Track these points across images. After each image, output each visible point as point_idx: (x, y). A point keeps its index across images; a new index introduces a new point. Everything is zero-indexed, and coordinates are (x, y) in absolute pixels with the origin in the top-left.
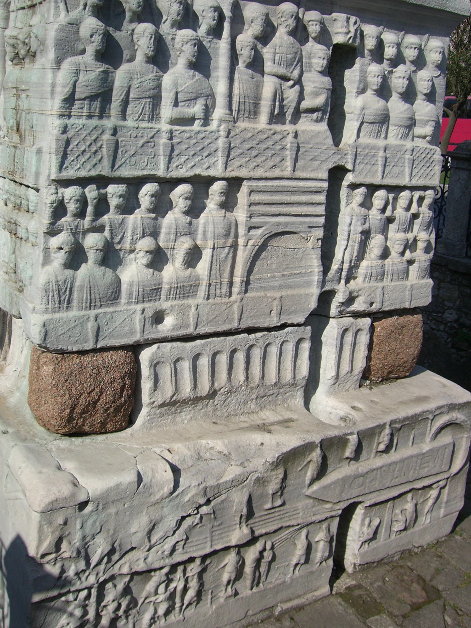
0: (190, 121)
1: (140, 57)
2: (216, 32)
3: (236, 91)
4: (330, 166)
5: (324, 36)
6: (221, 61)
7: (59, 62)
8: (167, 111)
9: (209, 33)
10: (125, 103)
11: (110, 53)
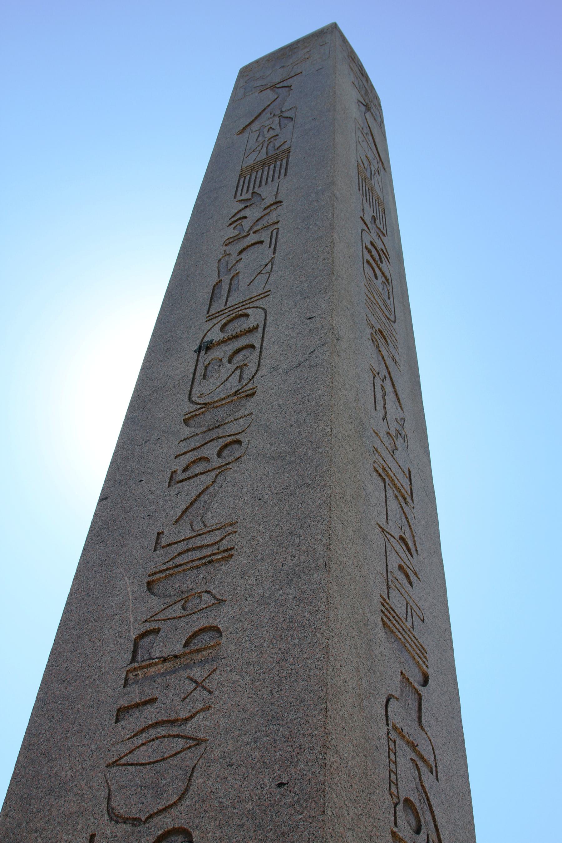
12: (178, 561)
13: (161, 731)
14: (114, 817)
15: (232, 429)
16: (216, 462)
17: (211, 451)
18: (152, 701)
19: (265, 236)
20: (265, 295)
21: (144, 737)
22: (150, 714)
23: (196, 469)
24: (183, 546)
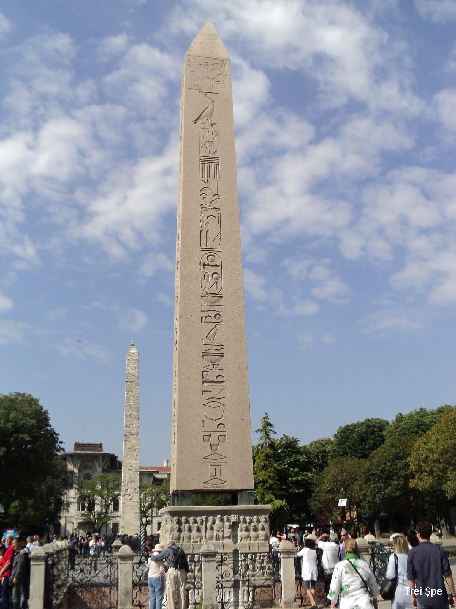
0: (197, 542)
1: (186, 531)
2: (202, 524)
3: (207, 535)
4: (233, 549)
5: (228, 520)
6: (203, 529)
7: (170, 533)
8: (192, 540)
9: (201, 524)
10: (183, 539)
11: (180, 530)
13: (213, 400)
15: (217, 309)
16: (214, 320)
17: (212, 314)
18: (211, 391)
22: (210, 395)
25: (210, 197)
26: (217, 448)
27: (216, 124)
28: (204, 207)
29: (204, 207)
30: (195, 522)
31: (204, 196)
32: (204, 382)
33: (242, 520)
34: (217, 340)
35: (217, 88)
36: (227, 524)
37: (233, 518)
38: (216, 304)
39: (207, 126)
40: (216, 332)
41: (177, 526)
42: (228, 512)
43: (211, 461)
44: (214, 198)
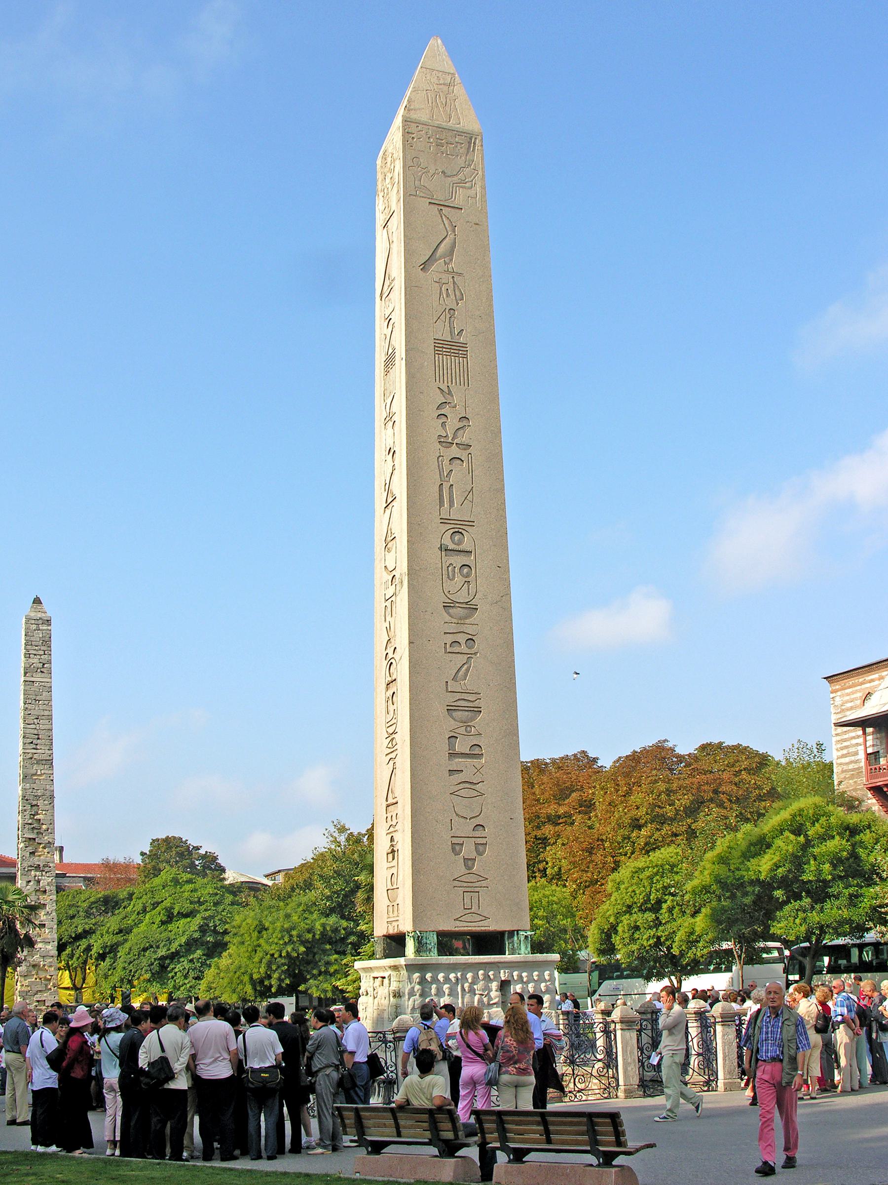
3: (465, 1000)
12: (458, 703)
13: (467, 785)
14: (457, 815)
15: (470, 629)
17: (462, 638)
19: (463, 455)
20: (471, 523)
21: (462, 786)
23: (456, 649)
24: (458, 696)
25: (453, 423)
26: (473, 865)
27: (460, 274)
28: (444, 442)
29: (444, 442)
30: (447, 980)
31: (443, 419)
32: (453, 755)
33: (515, 978)
34: (469, 683)
35: (460, 198)
36: (494, 985)
37: (503, 975)
38: (467, 621)
39: (446, 277)
40: (468, 670)
41: (417, 987)
42: (496, 966)
43: (465, 884)
44: (461, 425)
